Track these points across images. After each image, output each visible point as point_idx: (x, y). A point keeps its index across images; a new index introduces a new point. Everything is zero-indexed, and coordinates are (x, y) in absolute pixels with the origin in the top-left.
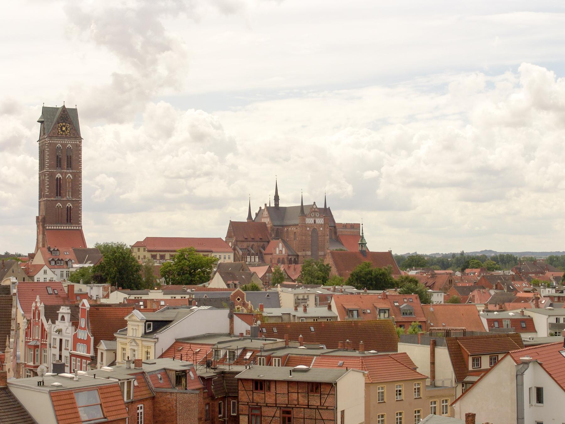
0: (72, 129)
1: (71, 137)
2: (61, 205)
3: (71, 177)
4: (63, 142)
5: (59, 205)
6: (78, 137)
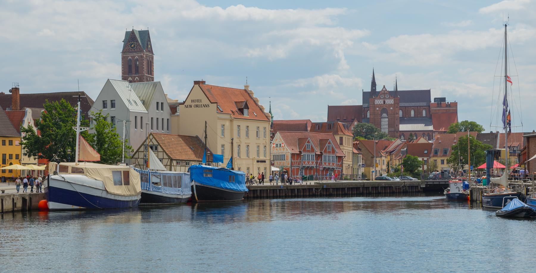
1: (138, 51)
3: (138, 79)
4: (133, 55)
6: (142, 51)
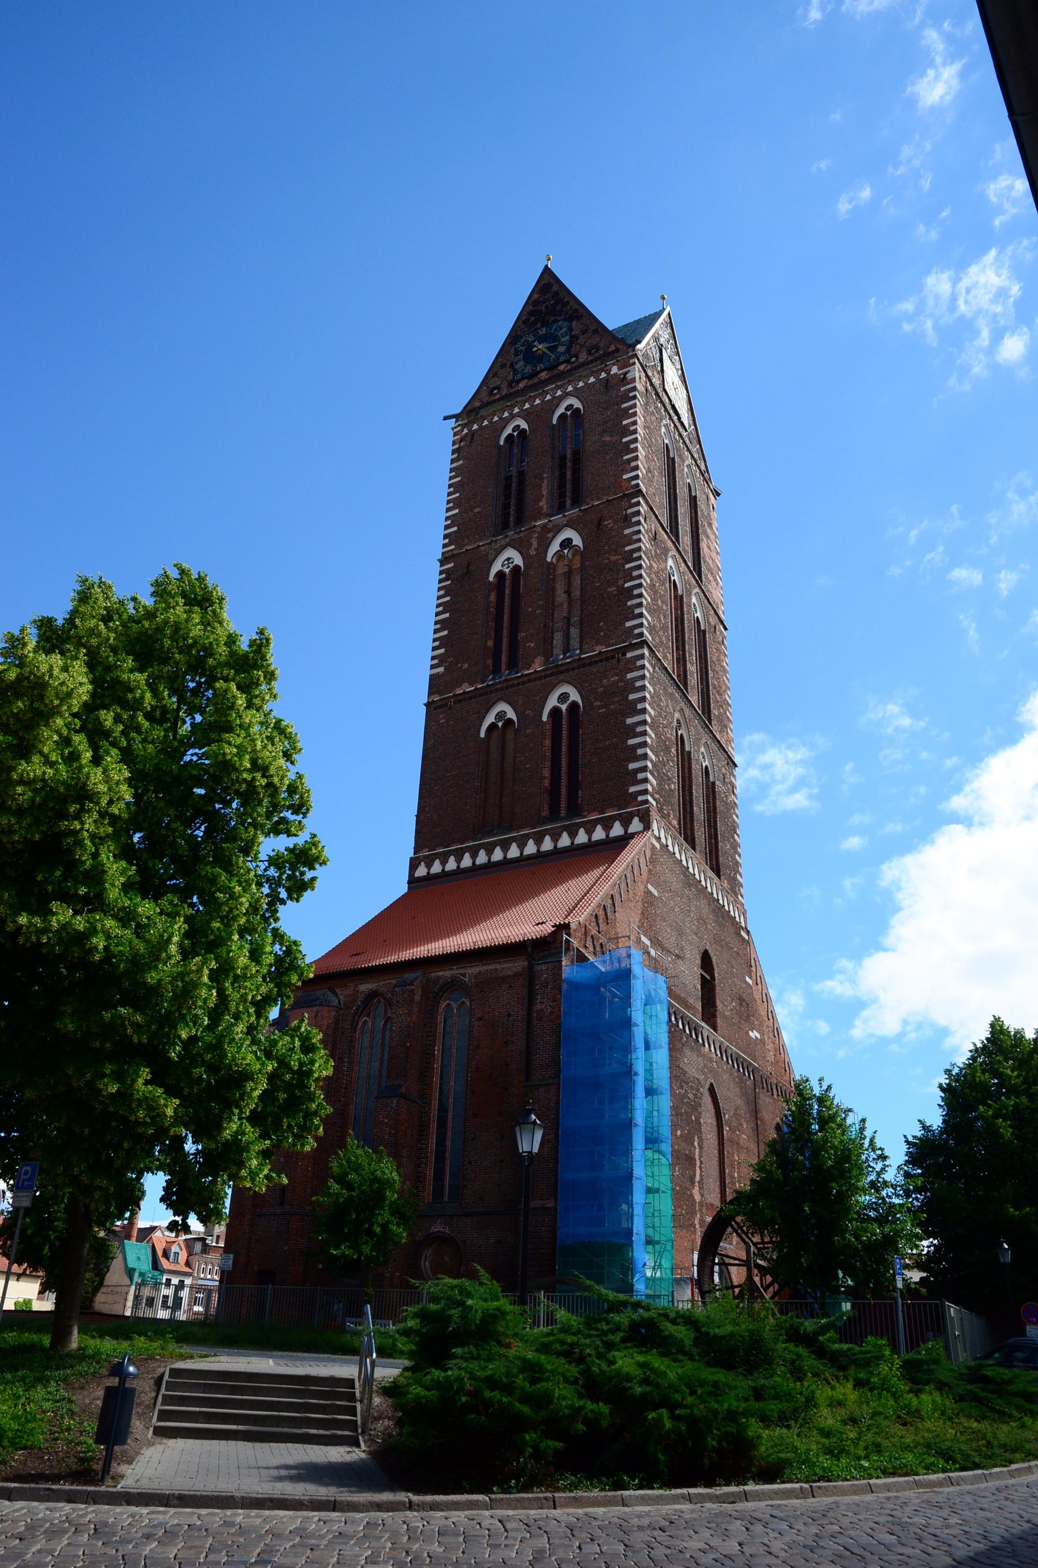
0: (584, 332)
2: (511, 714)
3: (577, 541)
5: (501, 715)
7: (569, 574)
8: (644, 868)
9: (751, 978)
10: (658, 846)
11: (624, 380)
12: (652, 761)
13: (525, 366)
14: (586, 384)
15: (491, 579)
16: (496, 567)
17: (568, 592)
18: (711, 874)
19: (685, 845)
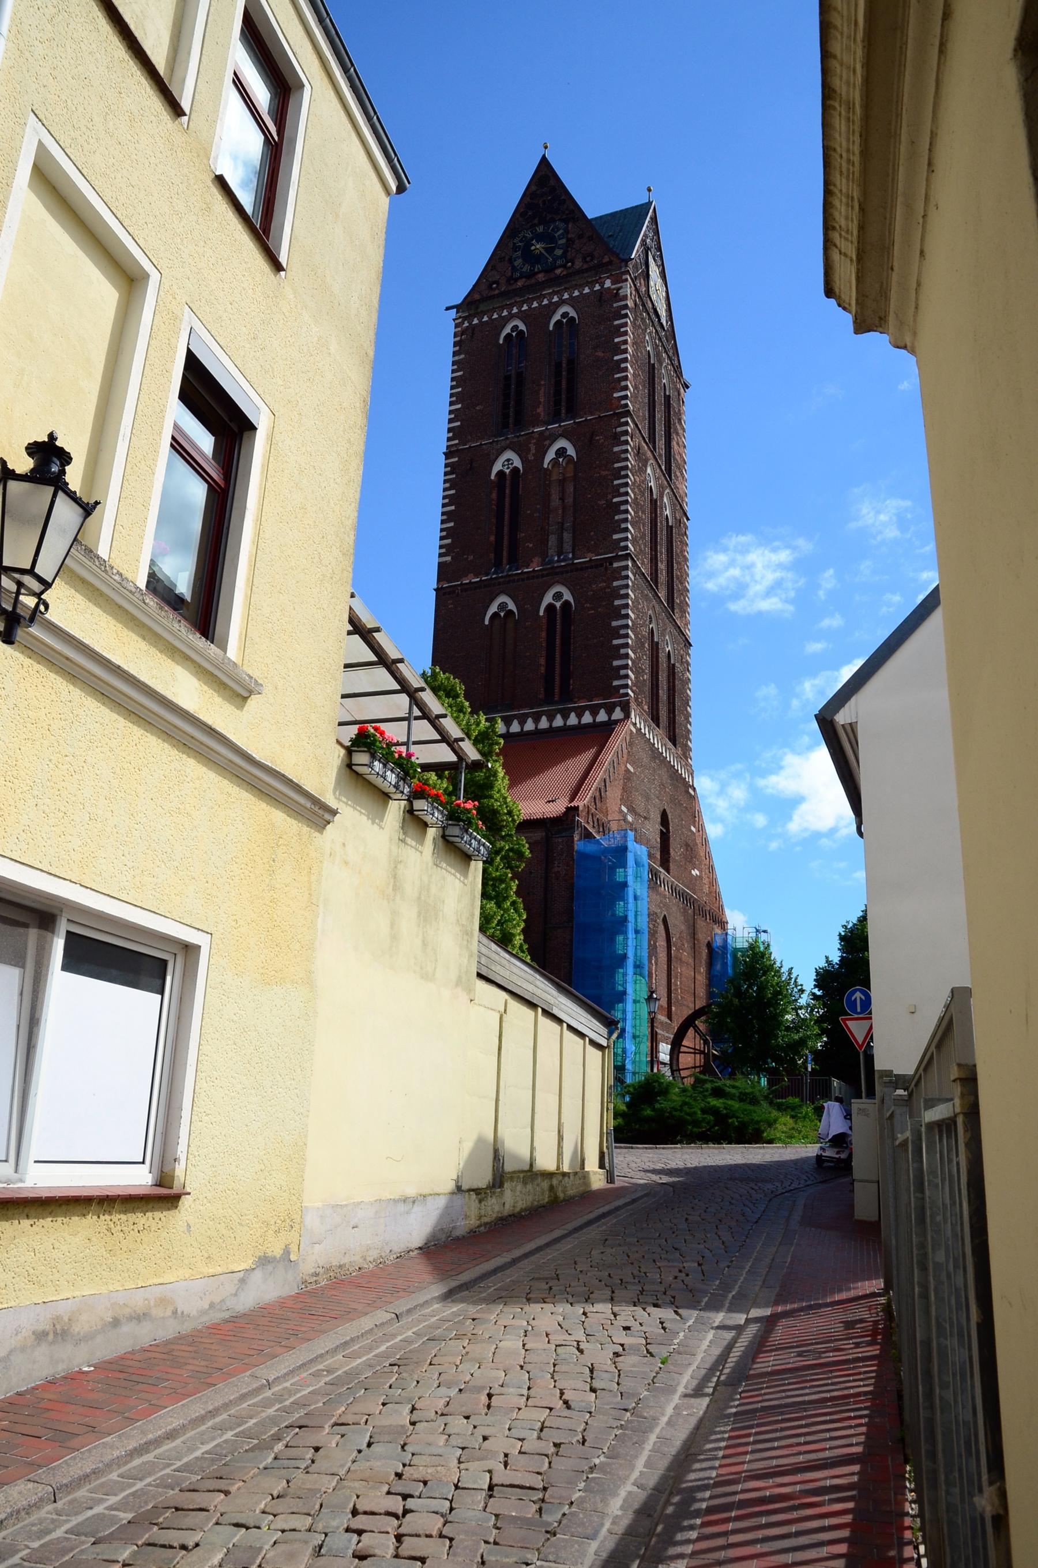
0: (580, 237)
2: (512, 606)
3: (571, 451)
5: (503, 606)
7: (562, 482)
8: (625, 751)
9: (694, 827)
10: (634, 730)
11: (616, 296)
12: (631, 659)
13: (524, 265)
14: (581, 294)
15: (493, 477)
16: (497, 467)
17: (562, 499)
18: (670, 745)
19: (653, 725)
